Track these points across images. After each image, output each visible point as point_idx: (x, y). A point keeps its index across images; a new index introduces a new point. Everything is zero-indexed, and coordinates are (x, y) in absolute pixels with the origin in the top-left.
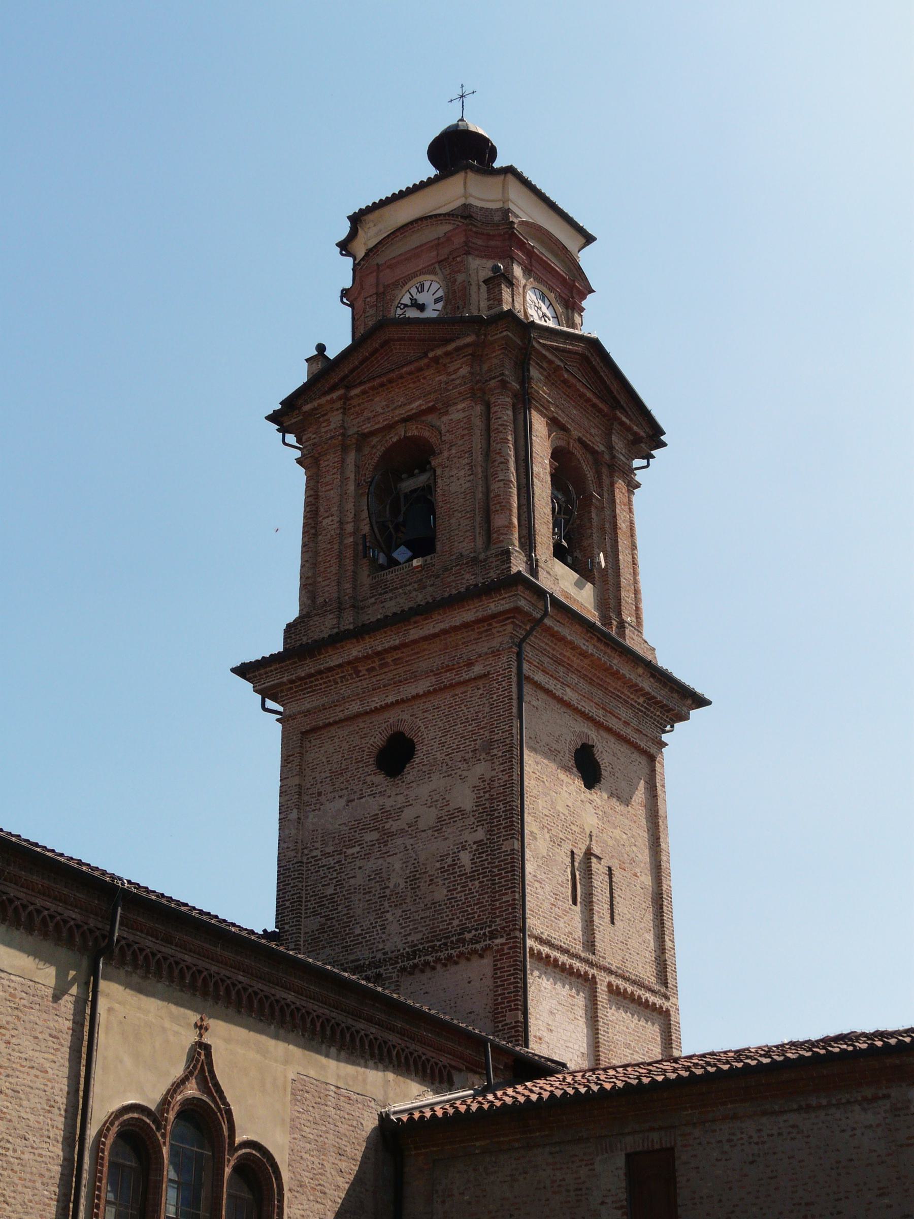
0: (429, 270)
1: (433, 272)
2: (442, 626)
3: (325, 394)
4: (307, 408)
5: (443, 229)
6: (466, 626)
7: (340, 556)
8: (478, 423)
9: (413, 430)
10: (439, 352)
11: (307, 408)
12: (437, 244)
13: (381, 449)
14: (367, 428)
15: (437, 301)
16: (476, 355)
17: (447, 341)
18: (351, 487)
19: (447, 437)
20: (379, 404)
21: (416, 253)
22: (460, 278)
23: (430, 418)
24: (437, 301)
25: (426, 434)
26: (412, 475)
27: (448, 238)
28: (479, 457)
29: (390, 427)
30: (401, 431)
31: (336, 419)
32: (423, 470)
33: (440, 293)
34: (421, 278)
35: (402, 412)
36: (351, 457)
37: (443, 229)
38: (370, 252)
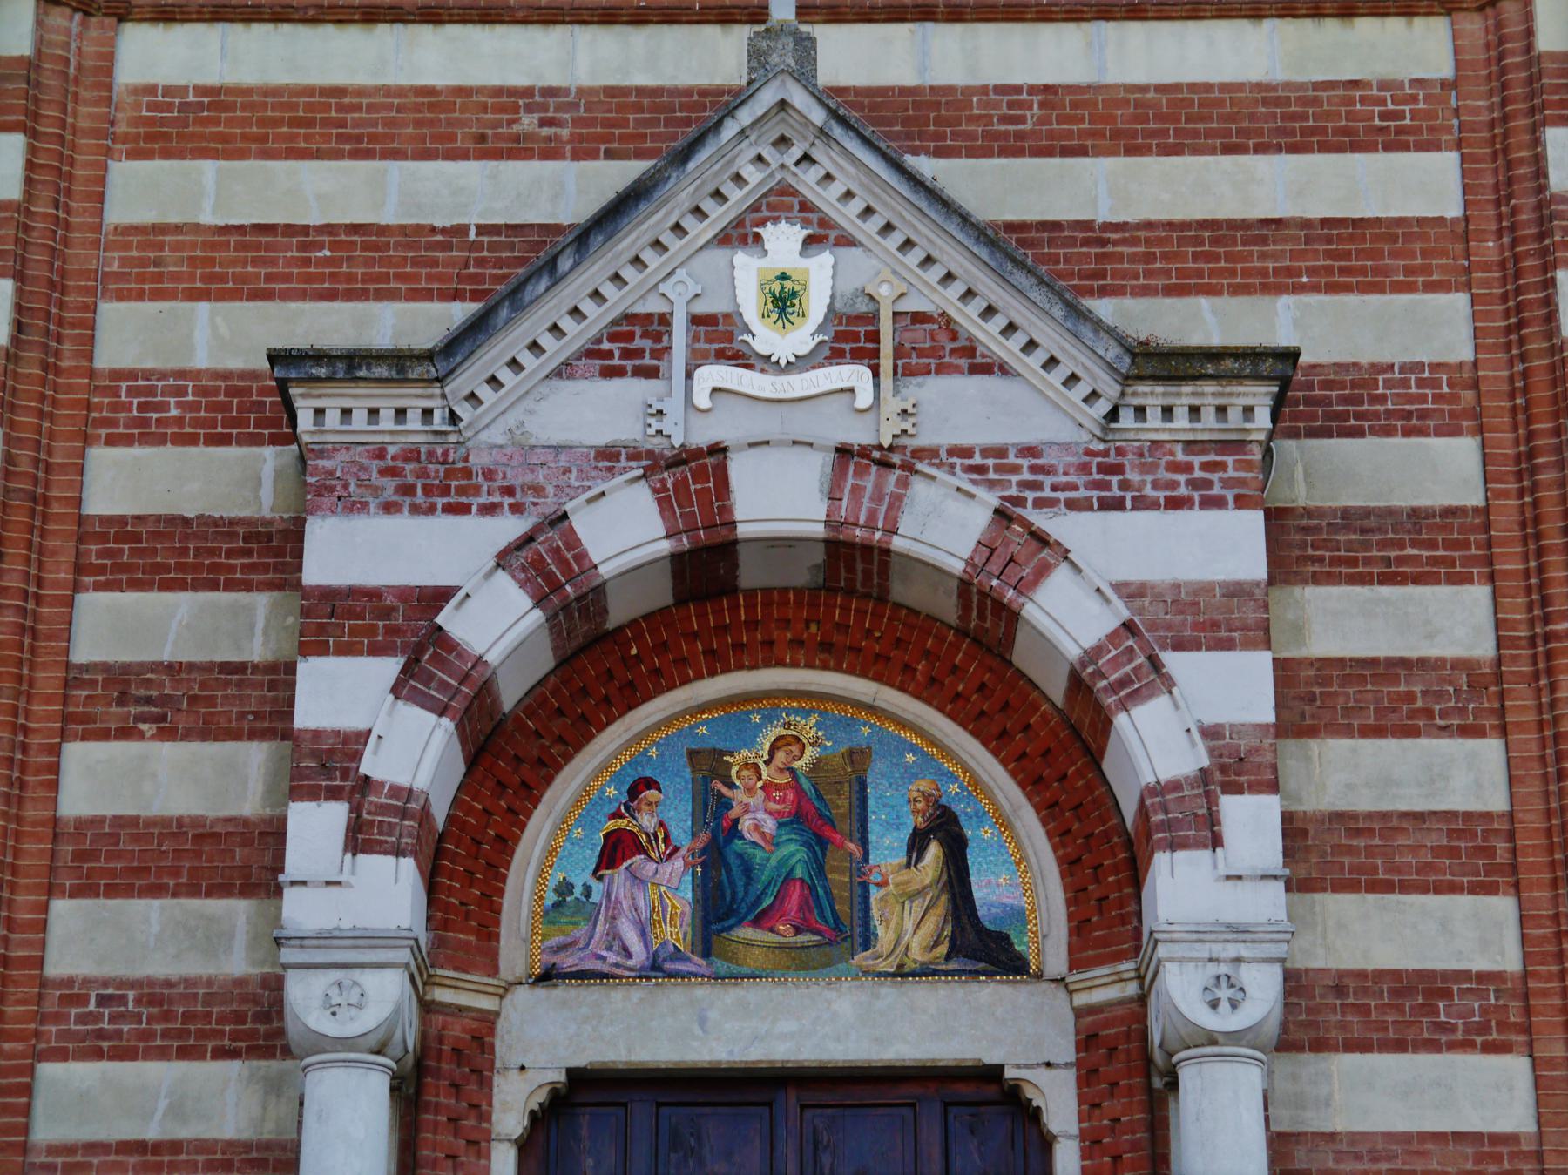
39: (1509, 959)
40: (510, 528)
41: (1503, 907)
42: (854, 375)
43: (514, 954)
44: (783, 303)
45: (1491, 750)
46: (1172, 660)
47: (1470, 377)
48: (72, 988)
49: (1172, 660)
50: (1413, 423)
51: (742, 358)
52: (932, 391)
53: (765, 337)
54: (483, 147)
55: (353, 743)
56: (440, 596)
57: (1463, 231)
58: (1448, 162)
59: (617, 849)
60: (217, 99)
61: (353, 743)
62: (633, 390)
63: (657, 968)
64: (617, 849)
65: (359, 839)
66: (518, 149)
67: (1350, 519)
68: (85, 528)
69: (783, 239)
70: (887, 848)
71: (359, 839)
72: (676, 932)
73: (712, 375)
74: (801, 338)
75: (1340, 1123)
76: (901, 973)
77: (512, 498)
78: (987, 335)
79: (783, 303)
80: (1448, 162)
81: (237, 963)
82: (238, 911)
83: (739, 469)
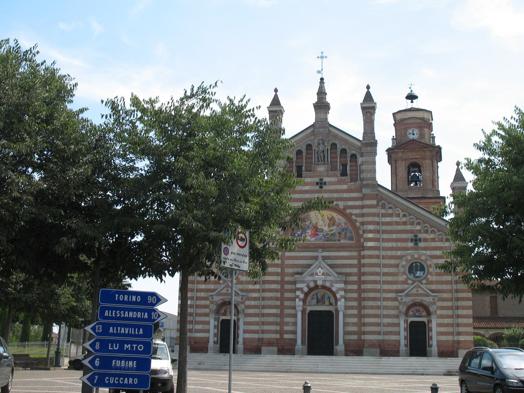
0: (415, 127)
1: (416, 128)
2: (428, 201)
3: (399, 149)
4: (395, 151)
5: (419, 121)
6: (432, 202)
7: (403, 181)
8: (431, 164)
9: (416, 161)
10: (425, 149)
11: (395, 151)
12: (418, 123)
13: (409, 162)
14: (407, 157)
15: (417, 134)
16: (431, 151)
17: (428, 148)
18: (404, 168)
19: (424, 165)
20: (410, 154)
21: (413, 123)
22: (423, 132)
23: (420, 159)
24: (417, 134)
25: (419, 162)
26: (413, 168)
27: (421, 124)
28: (431, 171)
29: (411, 159)
30: (414, 160)
31: (400, 154)
32: (416, 168)
33: (417, 133)
34: (414, 128)
35: (415, 157)
36: (404, 163)
37: (419, 121)
38: (403, 120)
39: (357, 305)
40: (306, 284)
41: (357, 302)
42: (323, 276)
43: (307, 305)
44: (320, 272)
45: (357, 294)
46: (339, 292)
47: (357, 273)
48: (286, 306)
49: (339, 292)
50: (354, 276)
51: (318, 275)
52: (327, 277)
53: (319, 274)
54: (305, 259)
55: (299, 296)
56: (303, 288)
57: (357, 264)
58: (356, 261)
59: (312, 299)
60: (291, 256)
61: (299, 296)
62: (312, 277)
63: (314, 305)
64: (312, 299)
65: (299, 300)
66: (306, 259)
67: (350, 281)
68: (285, 281)
69: (320, 269)
70: (326, 299)
71: (299, 300)
72: (315, 303)
73: (316, 276)
74: (321, 274)
75: (348, 313)
76: (327, 305)
77: (306, 283)
78: (330, 274)
79: (320, 272)
80: (356, 261)
81: (293, 305)
82: (293, 302)
83: (318, 281)
